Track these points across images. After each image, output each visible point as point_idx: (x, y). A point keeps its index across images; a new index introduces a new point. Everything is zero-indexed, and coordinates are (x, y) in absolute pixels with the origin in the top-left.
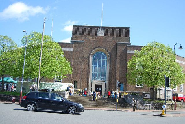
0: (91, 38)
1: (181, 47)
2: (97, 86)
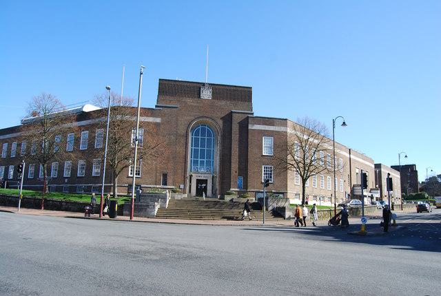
0: (189, 101)
1: (344, 123)
2: (199, 182)
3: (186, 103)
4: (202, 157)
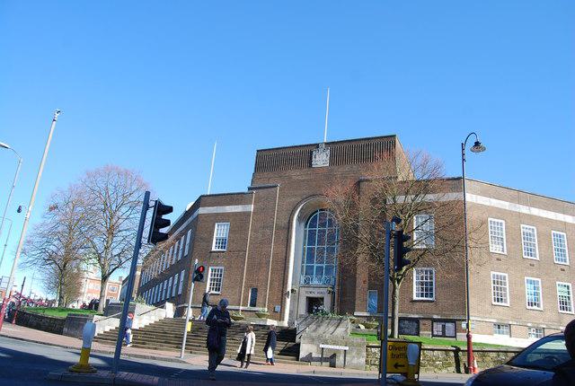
0: (296, 174)
3: (290, 178)
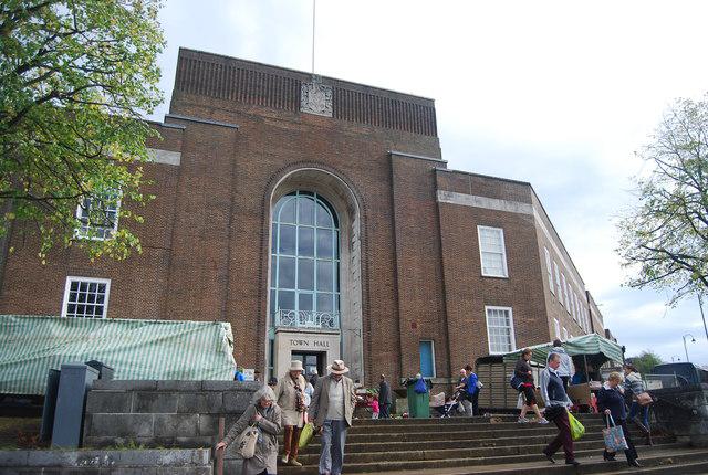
0: (268, 113)
4: (306, 283)
